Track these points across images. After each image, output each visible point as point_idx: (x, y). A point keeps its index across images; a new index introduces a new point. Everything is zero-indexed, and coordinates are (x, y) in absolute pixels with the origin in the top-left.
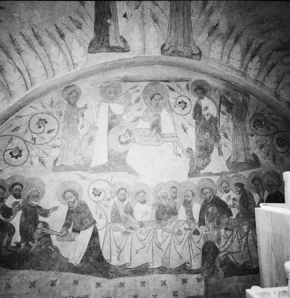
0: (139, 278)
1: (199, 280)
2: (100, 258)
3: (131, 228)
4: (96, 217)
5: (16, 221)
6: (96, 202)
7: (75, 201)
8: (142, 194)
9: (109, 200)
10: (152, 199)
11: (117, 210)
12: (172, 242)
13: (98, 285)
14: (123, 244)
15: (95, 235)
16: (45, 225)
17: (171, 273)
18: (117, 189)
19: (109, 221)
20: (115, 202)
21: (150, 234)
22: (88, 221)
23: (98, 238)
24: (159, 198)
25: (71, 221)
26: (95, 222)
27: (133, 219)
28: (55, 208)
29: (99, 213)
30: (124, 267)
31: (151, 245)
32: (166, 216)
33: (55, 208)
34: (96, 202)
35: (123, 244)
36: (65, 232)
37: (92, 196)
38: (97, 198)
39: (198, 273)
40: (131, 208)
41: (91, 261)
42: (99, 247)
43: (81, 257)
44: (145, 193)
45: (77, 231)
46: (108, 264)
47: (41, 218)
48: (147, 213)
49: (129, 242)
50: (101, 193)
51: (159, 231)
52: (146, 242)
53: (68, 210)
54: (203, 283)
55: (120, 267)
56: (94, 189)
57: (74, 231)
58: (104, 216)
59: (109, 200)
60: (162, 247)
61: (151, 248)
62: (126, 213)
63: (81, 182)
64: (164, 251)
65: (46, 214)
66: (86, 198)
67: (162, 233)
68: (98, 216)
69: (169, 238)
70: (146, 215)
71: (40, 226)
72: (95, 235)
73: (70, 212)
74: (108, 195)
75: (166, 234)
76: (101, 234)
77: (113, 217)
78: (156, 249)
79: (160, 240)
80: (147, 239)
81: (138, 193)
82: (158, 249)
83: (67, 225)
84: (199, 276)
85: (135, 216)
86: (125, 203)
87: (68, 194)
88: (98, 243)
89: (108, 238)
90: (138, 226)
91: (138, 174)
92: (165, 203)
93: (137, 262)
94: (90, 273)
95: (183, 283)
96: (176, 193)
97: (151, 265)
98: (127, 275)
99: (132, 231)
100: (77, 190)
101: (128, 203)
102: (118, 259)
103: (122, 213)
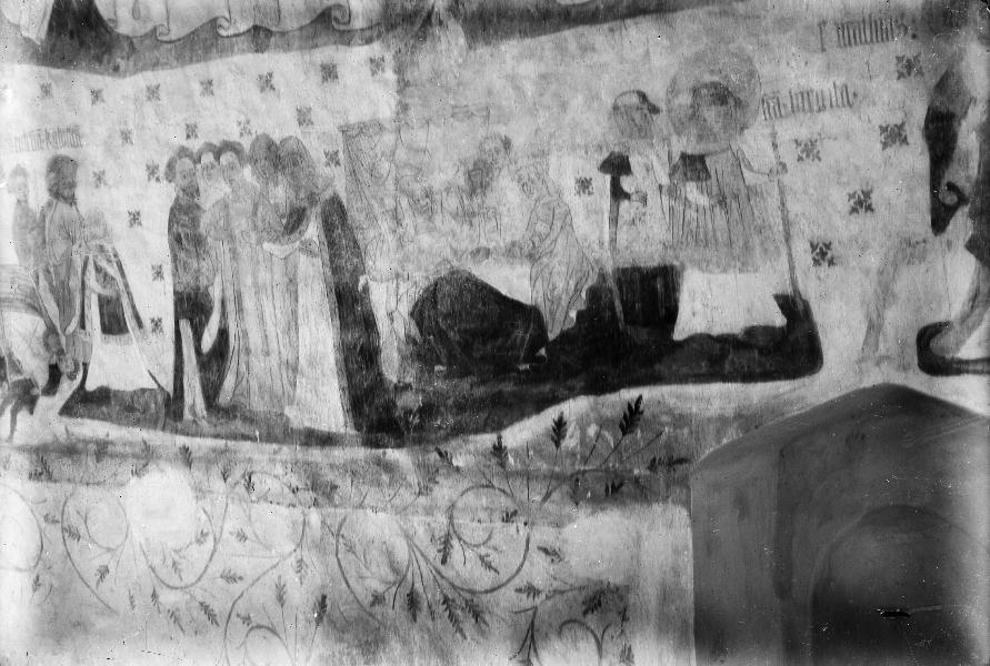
0: (196, 70)
1: (376, 65)
13: (96, 95)
17: (288, 47)
39: (369, 41)
41: (69, 27)
43: (48, 17)
54: (390, 75)
84: (376, 49)
95: (325, 79)
97: (225, 24)
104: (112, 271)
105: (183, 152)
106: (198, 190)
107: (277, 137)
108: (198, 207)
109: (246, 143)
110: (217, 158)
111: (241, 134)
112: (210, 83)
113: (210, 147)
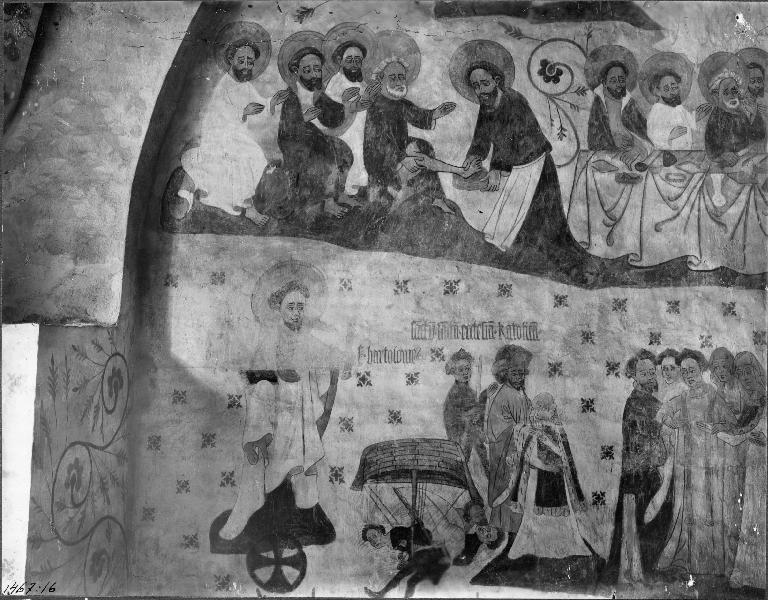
0: (667, 292)
2: (563, 237)
3: (641, 166)
4: (550, 134)
5: (354, 135)
6: (551, 97)
7: (495, 93)
8: (668, 80)
9: (581, 92)
10: (695, 95)
11: (605, 118)
12: (752, 210)
13: (560, 301)
14: (622, 202)
15: (548, 178)
16: (425, 147)
18: (601, 64)
19: (584, 146)
20: (597, 99)
21: (692, 184)
22: (529, 140)
23: (557, 187)
24: (715, 92)
25: (488, 141)
26: (548, 147)
27: (646, 143)
28: (447, 108)
29: (557, 124)
30: (624, 263)
31: (695, 212)
32: (734, 139)
33: (447, 108)
34: (551, 97)
35: (622, 202)
36: (472, 169)
37: (539, 80)
38: (549, 87)
40: (640, 116)
41: (540, 240)
42: (561, 209)
44: (678, 79)
45: (503, 166)
46: (584, 252)
47: (413, 131)
48: (681, 130)
49: (636, 199)
50: (560, 73)
51: (717, 178)
52: (680, 203)
53: (480, 114)
55: (614, 261)
56: (544, 63)
57: (495, 165)
58: (570, 132)
59: (581, 92)
60: (724, 219)
61: (694, 221)
62: (627, 126)
63: (509, 44)
64: (730, 229)
65: (425, 119)
66: (525, 84)
67: (723, 183)
68: (556, 131)
69: (743, 197)
70: (681, 134)
71: (411, 149)
72: (548, 178)
73: (483, 119)
74: (580, 80)
75: (732, 184)
76: (564, 177)
77: (591, 137)
78: (707, 222)
79: (718, 200)
80: (685, 197)
81: (658, 78)
82: (714, 224)
83: (478, 151)
85: (649, 134)
86: (625, 101)
87: (479, 74)
88: (558, 198)
89: (581, 188)
90: (659, 162)
91: (656, 27)
92: (731, 106)
93: (661, 248)
94: (537, 270)
96: (760, 80)
98: (633, 284)
99: (644, 174)
100: (499, 63)
101: (632, 102)
102: (609, 239)
103: (615, 125)
104: (558, 450)
105: (645, 354)
106: (656, 387)
107: (733, 350)
108: (656, 400)
109: (707, 353)
110: (678, 362)
111: (703, 346)
112: (677, 303)
113: (671, 353)
